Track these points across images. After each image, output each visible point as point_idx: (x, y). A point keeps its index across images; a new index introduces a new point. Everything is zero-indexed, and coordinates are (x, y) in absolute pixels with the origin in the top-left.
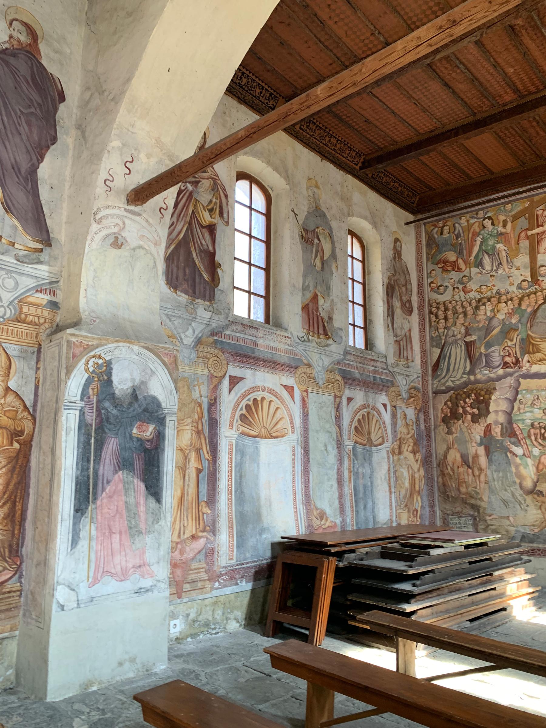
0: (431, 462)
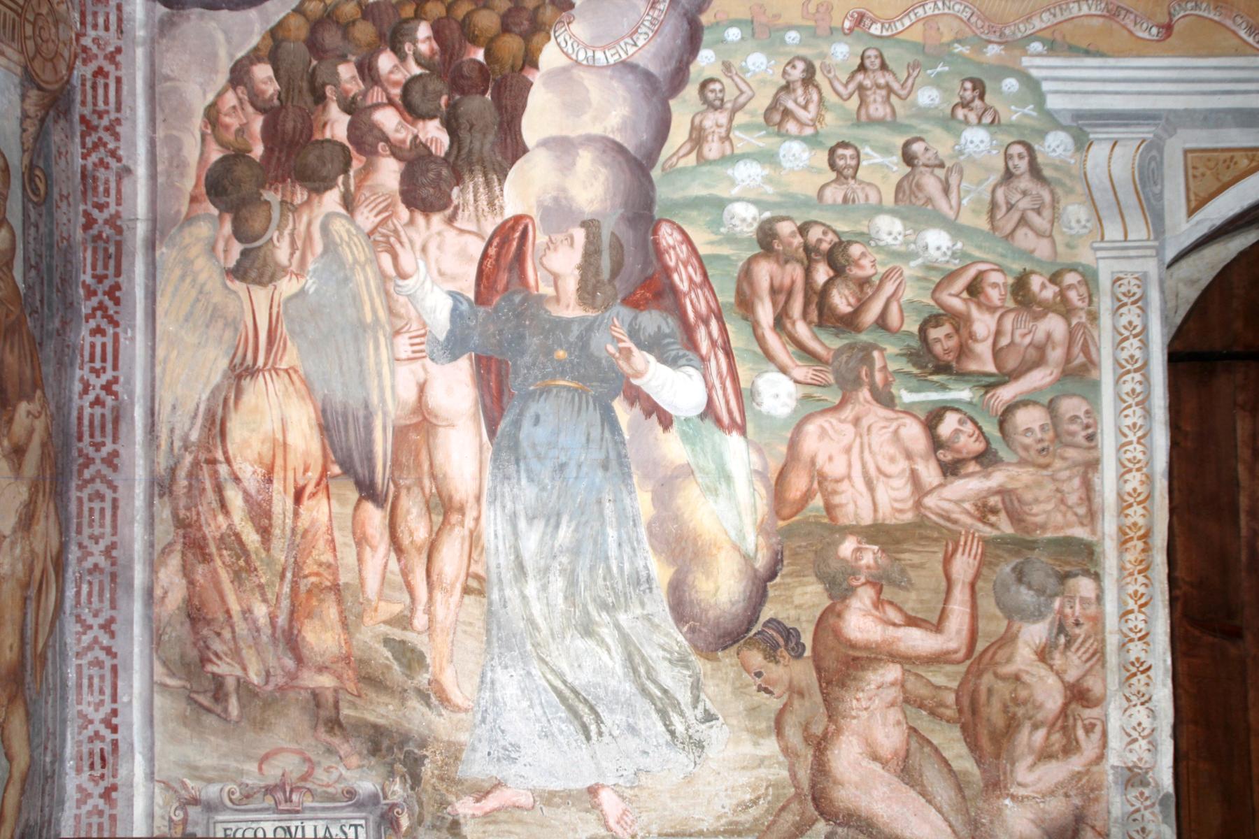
0: (111, 461)
